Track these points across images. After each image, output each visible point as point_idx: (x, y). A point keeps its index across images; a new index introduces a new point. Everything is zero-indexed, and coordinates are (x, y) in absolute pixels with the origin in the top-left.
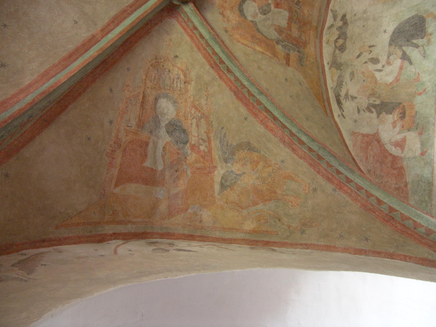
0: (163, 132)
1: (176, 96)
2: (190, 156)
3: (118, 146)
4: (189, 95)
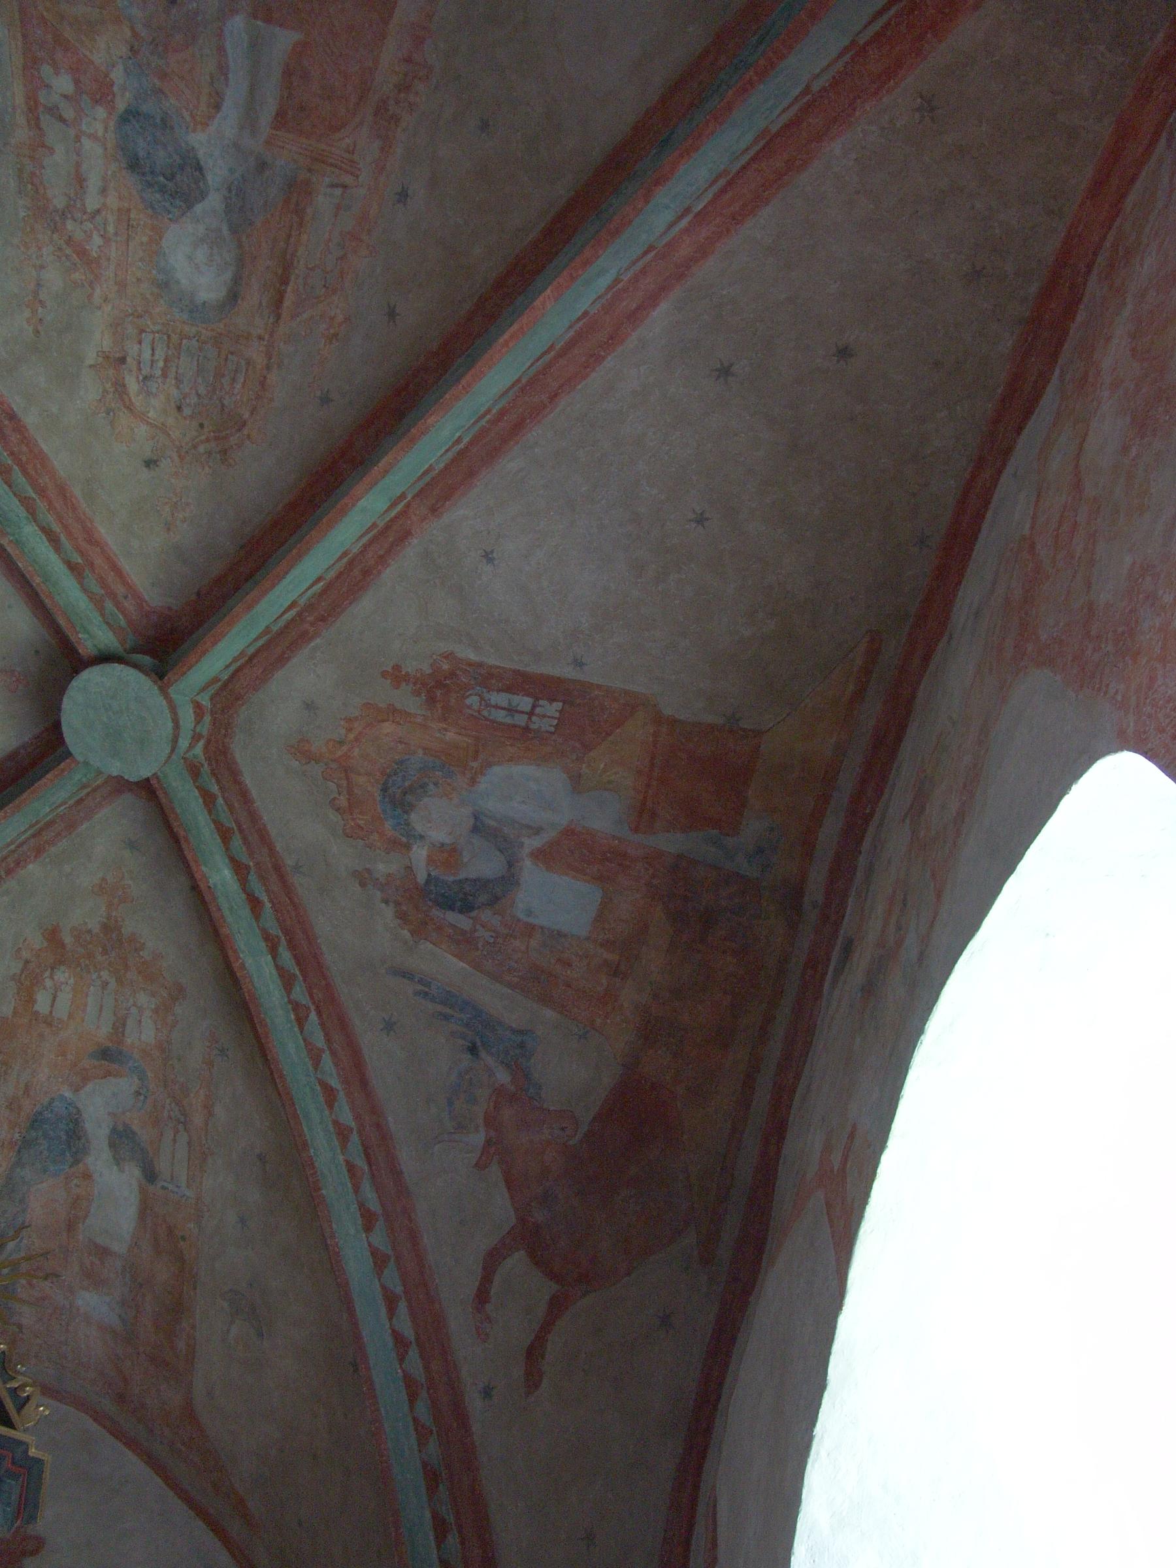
0: (217, 172)
1: (158, 310)
2: (114, 58)
3: (387, 110)
4: (108, 308)
